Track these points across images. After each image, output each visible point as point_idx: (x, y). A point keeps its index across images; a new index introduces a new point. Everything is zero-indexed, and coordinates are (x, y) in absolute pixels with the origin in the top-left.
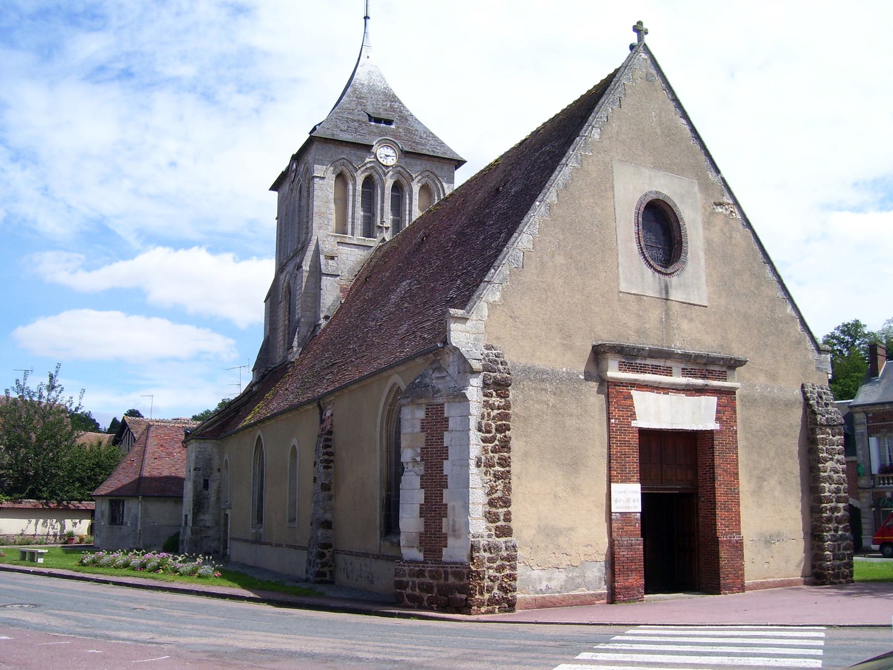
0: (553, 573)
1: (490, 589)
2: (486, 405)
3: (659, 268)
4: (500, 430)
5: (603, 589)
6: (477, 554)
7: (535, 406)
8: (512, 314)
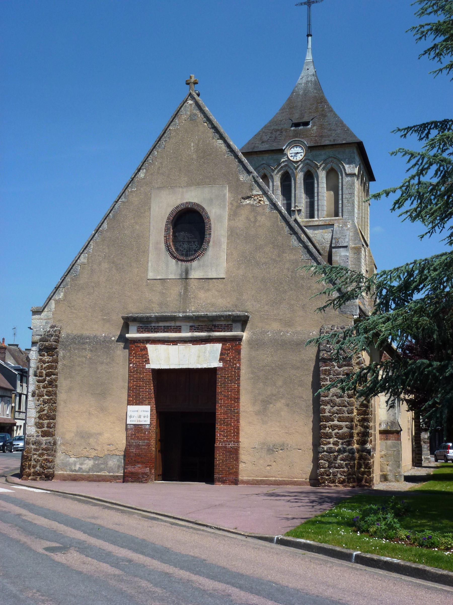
0: (85, 460)
1: (34, 467)
2: (41, 361)
3: (181, 258)
4: (48, 375)
5: (120, 473)
6: (28, 446)
7: (78, 359)
8: (70, 305)
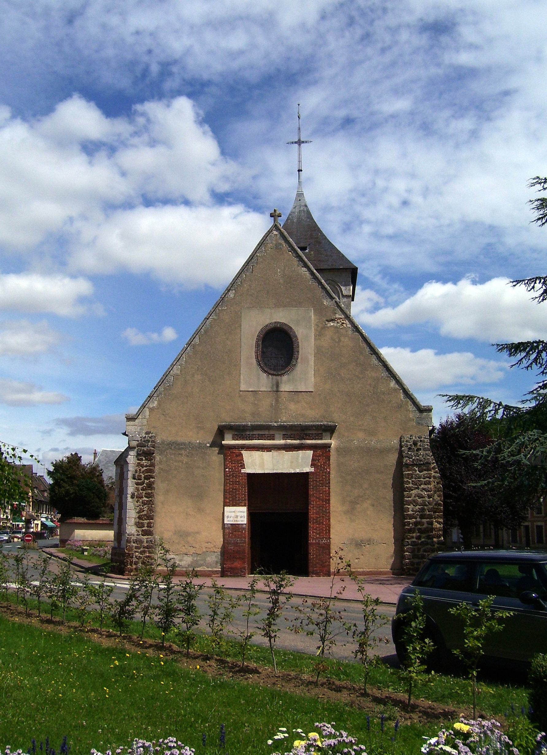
1: (136, 563)
2: (139, 465)
4: (146, 478)
